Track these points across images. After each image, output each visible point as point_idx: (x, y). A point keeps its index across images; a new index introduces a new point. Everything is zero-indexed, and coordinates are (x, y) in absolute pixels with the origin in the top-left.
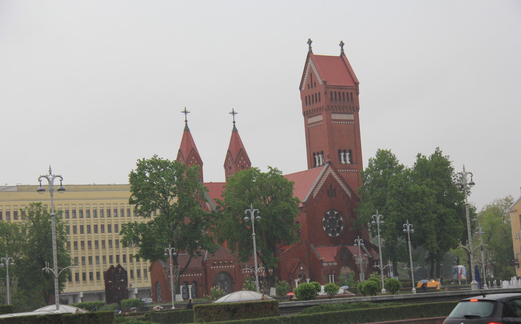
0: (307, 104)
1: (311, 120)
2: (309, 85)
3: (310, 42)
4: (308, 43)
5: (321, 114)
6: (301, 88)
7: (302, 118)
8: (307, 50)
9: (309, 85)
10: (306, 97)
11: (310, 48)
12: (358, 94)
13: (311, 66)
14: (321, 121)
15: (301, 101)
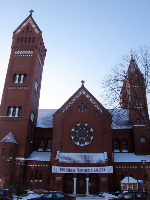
0: (18, 42)
1: (16, 52)
2: (24, 32)
3: (32, 11)
4: (30, 11)
5: (32, 50)
6: (14, 33)
7: (10, 50)
8: (30, 14)
9: (24, 32)
10: (18, 38)
11: (31, 14)
12: (45, 56)
13: (29, 23)
14: (31, 54)
15: (12, 40)
